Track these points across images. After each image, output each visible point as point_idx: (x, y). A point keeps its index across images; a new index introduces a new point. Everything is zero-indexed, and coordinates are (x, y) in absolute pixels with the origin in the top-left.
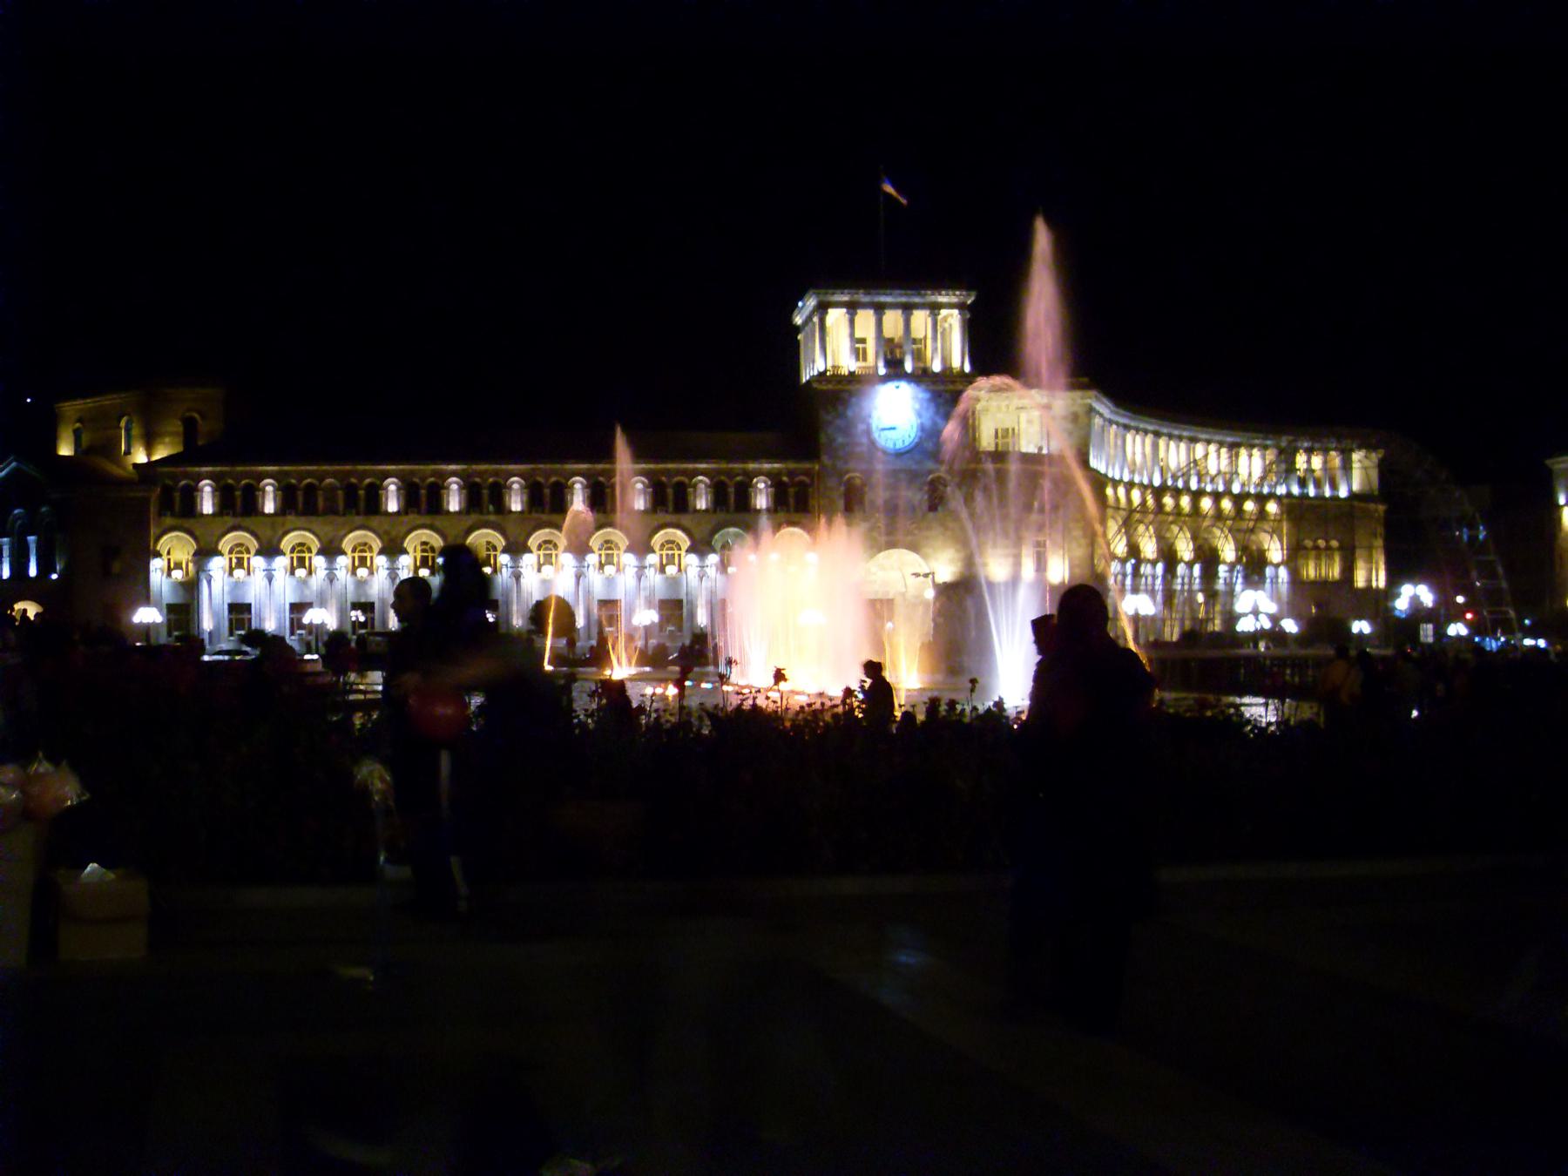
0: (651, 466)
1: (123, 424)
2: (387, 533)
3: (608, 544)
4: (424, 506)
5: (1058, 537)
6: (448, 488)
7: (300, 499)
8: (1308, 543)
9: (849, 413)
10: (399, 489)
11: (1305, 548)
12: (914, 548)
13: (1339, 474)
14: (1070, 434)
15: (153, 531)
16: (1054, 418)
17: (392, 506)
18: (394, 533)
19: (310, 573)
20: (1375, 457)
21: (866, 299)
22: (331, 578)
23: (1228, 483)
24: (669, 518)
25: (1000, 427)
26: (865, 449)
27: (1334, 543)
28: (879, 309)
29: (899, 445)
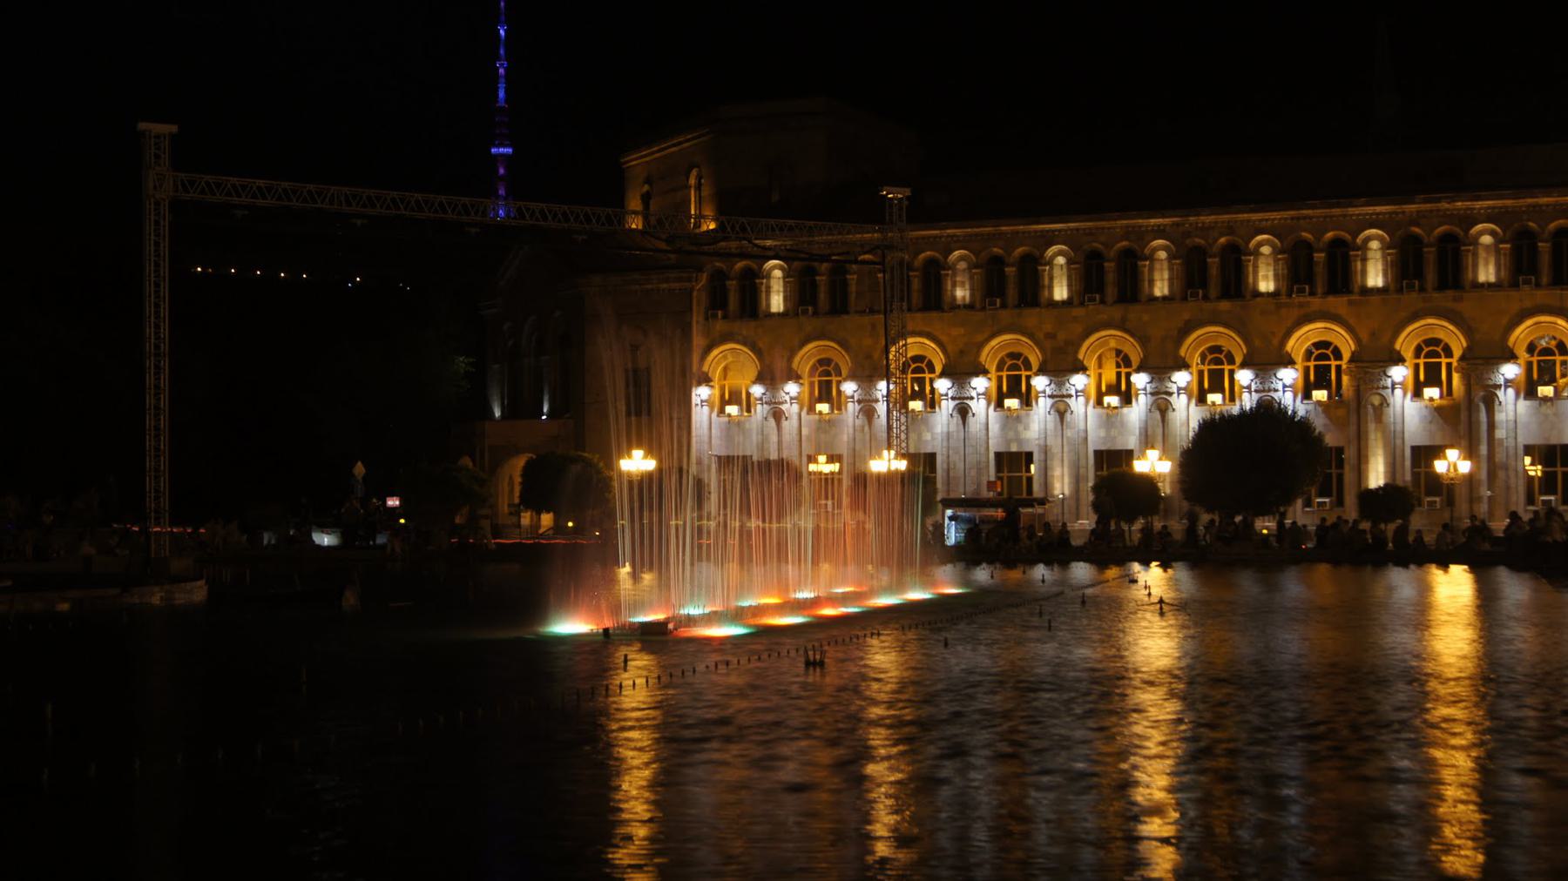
0: (1508, 202)
1: (692, 181)
2: (1051, 336)
3: (1431, 348)
4: (1111, 292)
6: (1151, 258)
7: (916, 284)
10: (1070, 262)
15: (698, 341)
17: (1060, 292)
18: (1061, 336)
19: (932, 404)
22: (963, 411)
24: (1541, 296)
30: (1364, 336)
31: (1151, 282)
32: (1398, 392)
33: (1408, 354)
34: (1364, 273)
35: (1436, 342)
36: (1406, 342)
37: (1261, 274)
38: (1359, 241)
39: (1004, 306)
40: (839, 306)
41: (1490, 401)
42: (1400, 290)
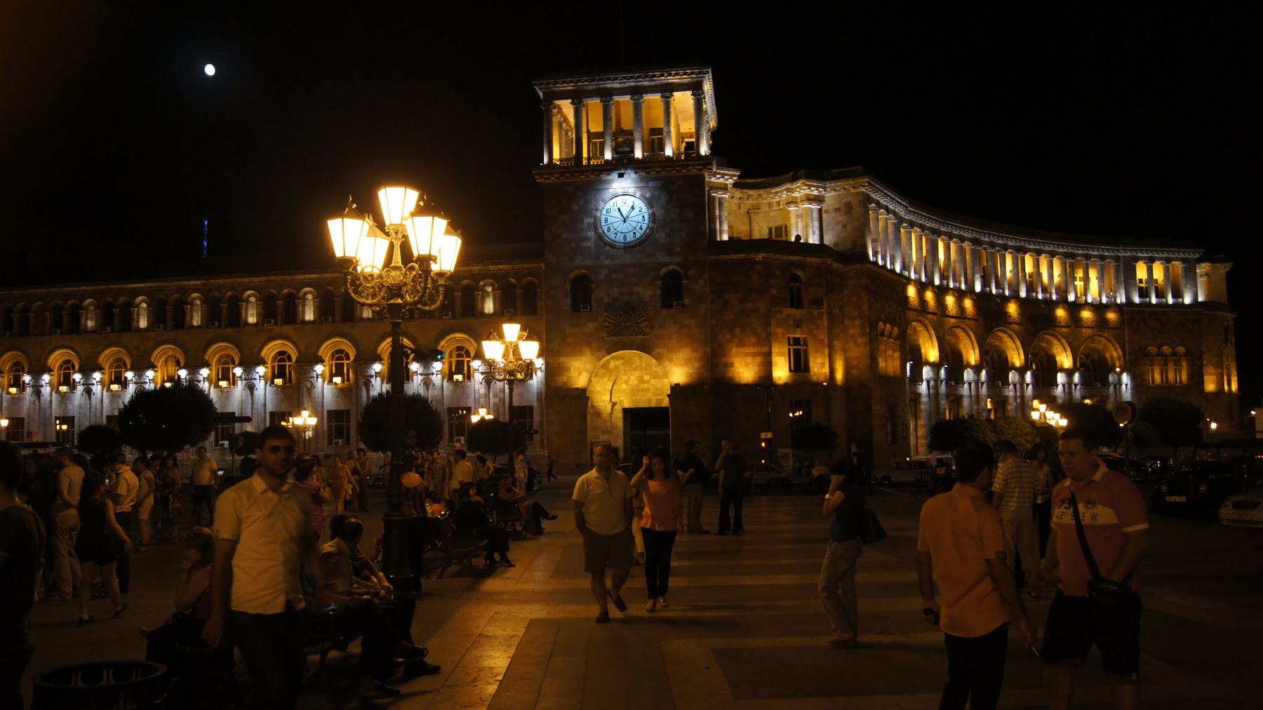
3: (339, 354)
4: (170, 323)
5: (823, 336)
6: (192, 304)
8: (1152, 350)
9: (575, 207)
11: (1147, 355)
12: (646, 348)
13: (1182, 282)
14: (844, 226)
16: (827, 211)
17: (143, 323)
20: (1223, 269)
21: (592, 86)
22: (88, 392)
23: (1063, 292)
25: (774, 225)
26: (591, 244)
27: (1181, 350)
28: (606, 95)
29: (630, 238)
30: (302, 348)
31: (192, 318)
32: (320, 380)
33: (327, 359)
34: (303, 312)
35: (341, 351)
36: (325, 350)
37: (250, 312)
38: (301, 294)
39: (112, 331)
40: (25, 332)
41: (368, 384)
42: (321, 323)
